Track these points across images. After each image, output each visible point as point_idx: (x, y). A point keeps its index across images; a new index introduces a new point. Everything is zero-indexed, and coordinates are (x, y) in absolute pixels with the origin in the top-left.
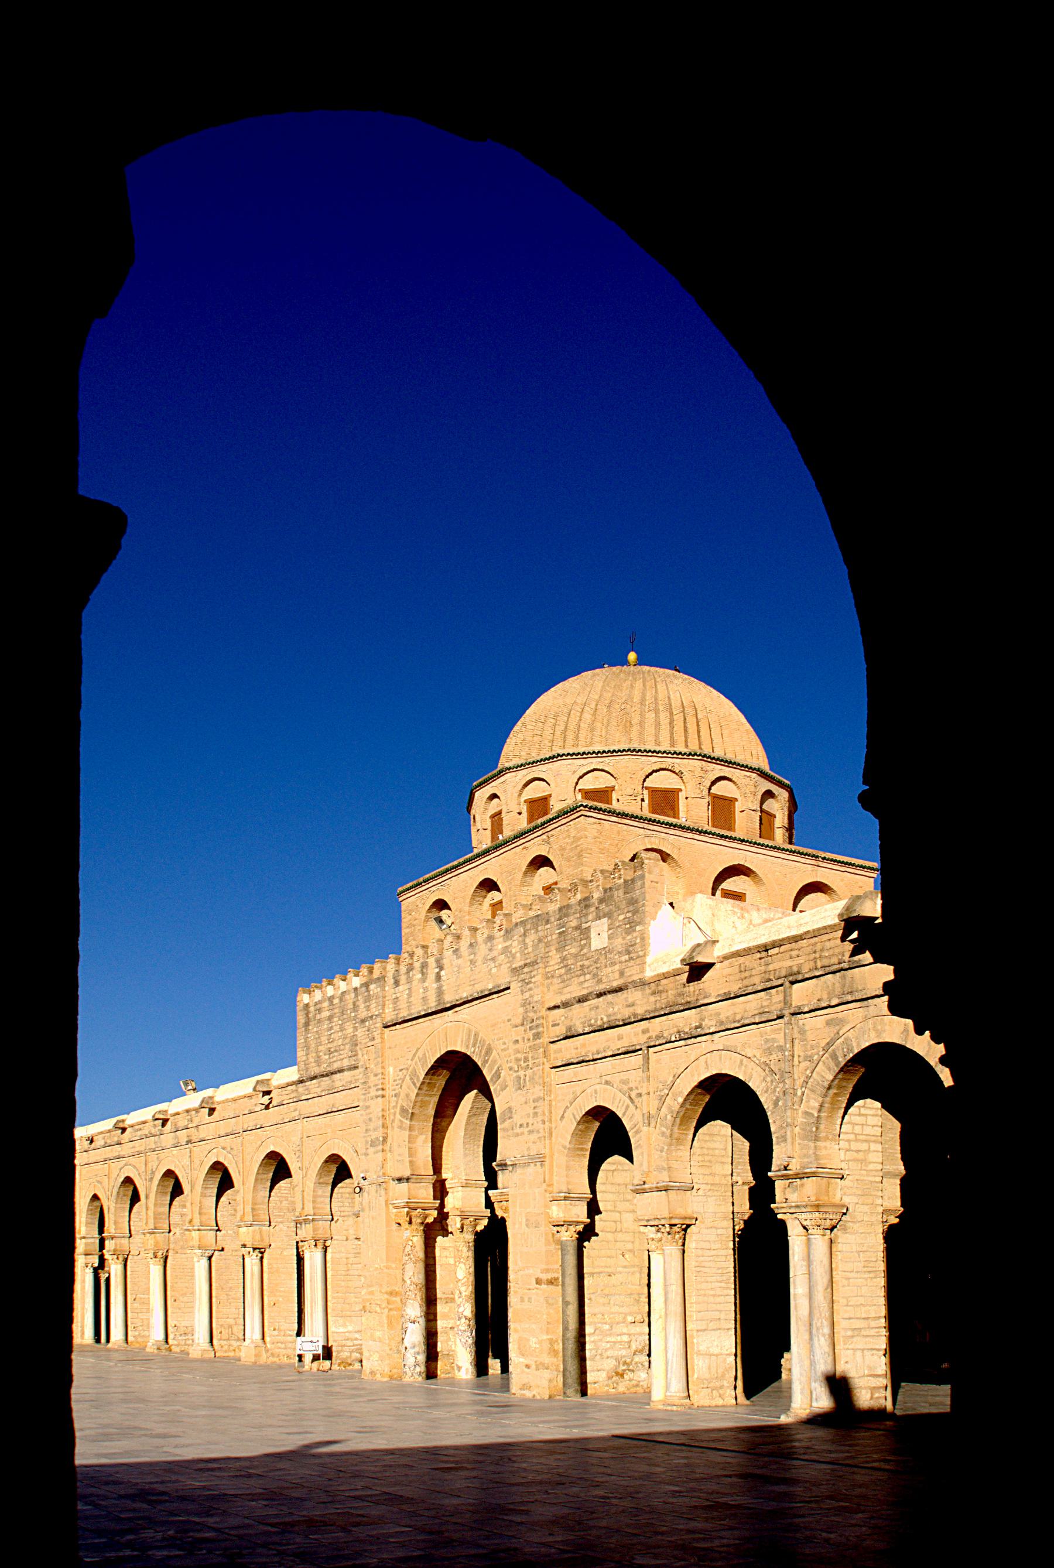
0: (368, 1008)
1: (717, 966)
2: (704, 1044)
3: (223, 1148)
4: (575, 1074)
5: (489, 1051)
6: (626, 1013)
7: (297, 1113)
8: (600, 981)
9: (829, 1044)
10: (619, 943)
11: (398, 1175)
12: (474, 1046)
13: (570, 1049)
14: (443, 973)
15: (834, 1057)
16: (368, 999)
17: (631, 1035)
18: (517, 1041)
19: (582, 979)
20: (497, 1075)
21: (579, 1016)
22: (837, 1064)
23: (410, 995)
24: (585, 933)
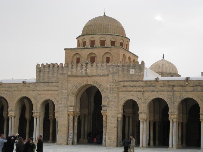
0: (63, 72)
1: (159, 82)
2: (155, 93)
3: (4, 94)
4: (125, 93)
5: (100, 85)
6: (138, 85)
7: (35, 89)
8: (132, 79)
9: (179, 97)
10: (137, 74)
11: (70, 105)
12: (96, 84)
13: (124, 89)
14: (87, 69)
15: (181, 98)
16: (63, 70)
17: (138, 89)
18: (111, 86)
19: (128, 78)
20: (103, 90)
21: (126, 84)
22: (181, 99)
23: (76, 72)
24: (129, 71)
